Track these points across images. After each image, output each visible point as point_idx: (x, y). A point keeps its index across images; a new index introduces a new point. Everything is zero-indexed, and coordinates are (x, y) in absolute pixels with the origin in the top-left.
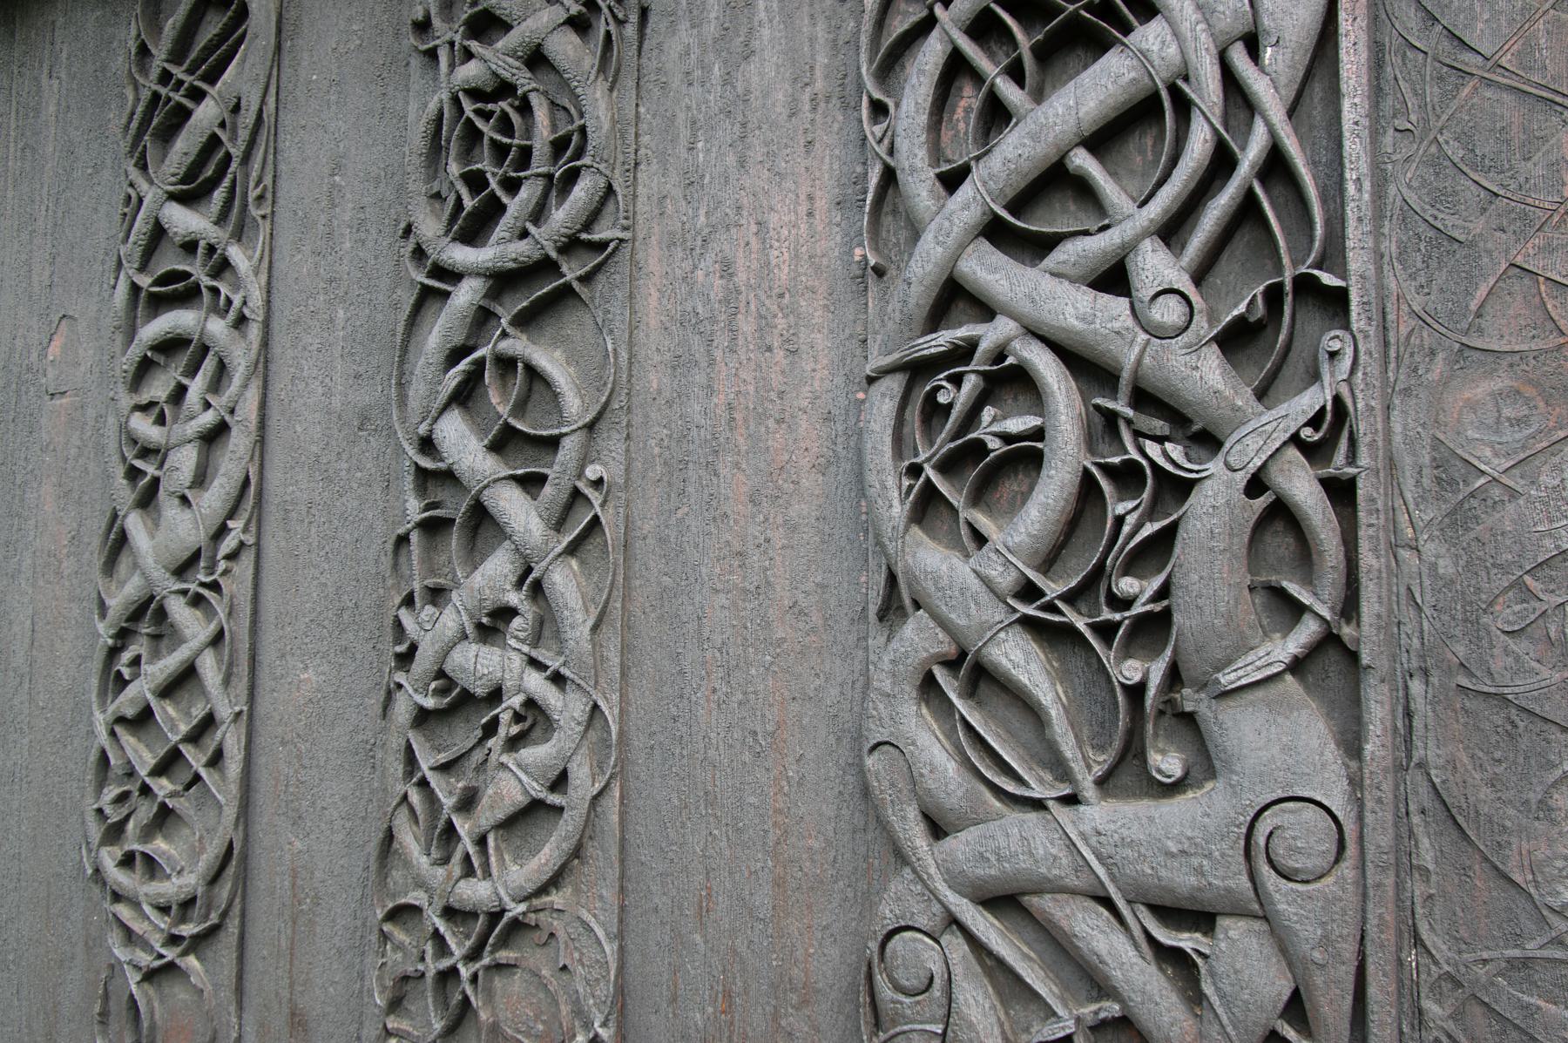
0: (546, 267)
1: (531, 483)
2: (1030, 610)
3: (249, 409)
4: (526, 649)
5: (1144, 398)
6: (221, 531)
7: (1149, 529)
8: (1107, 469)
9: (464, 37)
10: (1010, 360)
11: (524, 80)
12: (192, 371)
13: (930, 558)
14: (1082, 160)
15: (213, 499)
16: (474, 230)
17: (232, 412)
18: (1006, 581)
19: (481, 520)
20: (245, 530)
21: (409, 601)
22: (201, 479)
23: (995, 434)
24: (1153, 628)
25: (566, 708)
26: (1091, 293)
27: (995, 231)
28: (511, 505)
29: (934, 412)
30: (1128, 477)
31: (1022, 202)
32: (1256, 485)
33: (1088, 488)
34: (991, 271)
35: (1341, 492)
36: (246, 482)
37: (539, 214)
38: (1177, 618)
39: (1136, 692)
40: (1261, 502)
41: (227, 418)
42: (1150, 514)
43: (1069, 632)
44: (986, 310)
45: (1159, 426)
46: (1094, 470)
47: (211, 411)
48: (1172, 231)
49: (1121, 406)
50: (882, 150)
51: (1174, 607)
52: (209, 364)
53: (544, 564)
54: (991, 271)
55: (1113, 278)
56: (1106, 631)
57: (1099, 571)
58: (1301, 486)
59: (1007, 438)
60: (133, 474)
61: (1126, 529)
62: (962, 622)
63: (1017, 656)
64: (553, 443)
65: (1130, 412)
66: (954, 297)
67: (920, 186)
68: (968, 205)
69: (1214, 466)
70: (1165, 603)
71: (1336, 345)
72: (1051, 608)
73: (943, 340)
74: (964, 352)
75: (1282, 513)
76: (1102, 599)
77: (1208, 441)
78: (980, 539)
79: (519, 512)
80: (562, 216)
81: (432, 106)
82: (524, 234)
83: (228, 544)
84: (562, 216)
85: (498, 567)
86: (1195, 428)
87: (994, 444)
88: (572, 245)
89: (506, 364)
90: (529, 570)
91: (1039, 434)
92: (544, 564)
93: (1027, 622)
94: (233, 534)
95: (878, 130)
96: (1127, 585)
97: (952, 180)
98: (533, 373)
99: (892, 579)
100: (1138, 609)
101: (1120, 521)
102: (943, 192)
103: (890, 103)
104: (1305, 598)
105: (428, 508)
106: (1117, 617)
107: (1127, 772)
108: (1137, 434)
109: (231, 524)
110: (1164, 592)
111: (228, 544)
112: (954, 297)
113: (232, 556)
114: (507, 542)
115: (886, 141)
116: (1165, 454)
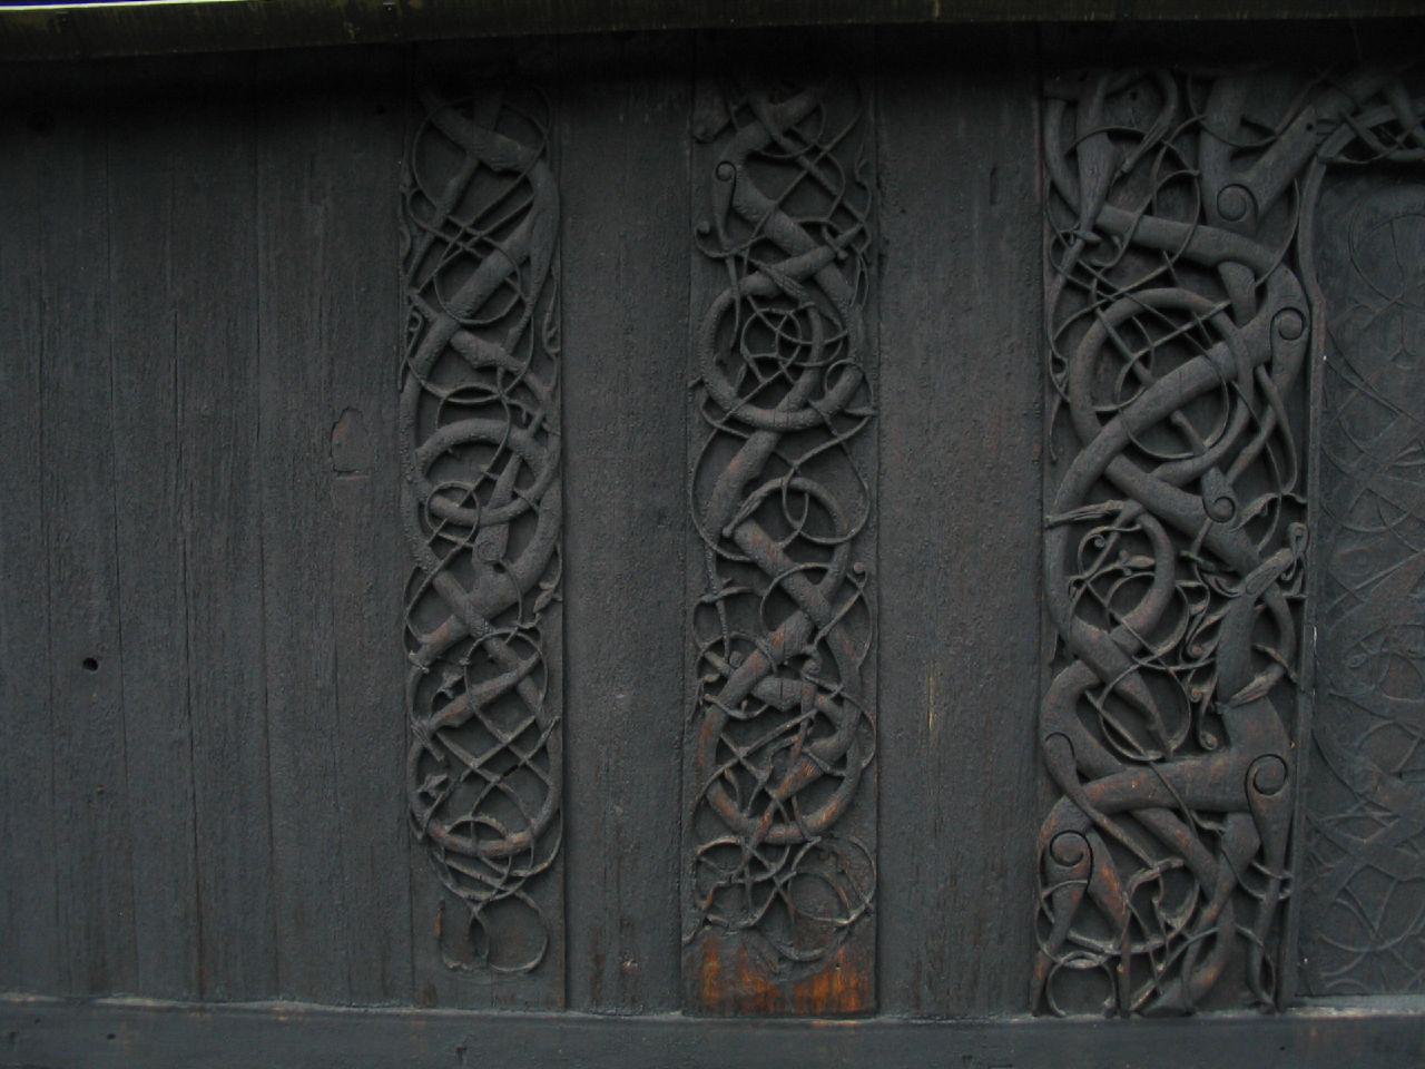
0: (821, 429)
1: (816, 574)
2: (1144, 662)
3: (553, 498)
4: (817, 681)
5: (1206, 551)
6: (535, 590)
7: (1207, 623)
8: (1187, 589)
9: (751, 254)
10: (1138, 527)
11: (807, 301)
12: (497, 467)
13: (1088, 631)
14: (1179, 418)
15: (526, 562)
16: (765, 399)
17: (538, 503)
18: (1133, 646)
19: (783, 599)
20: (556, 590)
21: (718, 647)
22: (511, 550)
23: (1129, 567)
24: (1205, 673)
25: (846, 717)
26: (1183, 494)
27: (1130, 450)
28: (800, 587)
29: (1092, 550)
30: (1197, 594)
31: (1144, 433)
32: (1260, 600)
33: (1176, 602)
34: (1123, 469)
35: (1295, 604)
36: (555, 553)
37: (817, 392)
38: (1220, 668)
39: (1196, 706)
40: (1260, 607)
41: (536, 507)
42: (1210, 611)
43: (1165, 674)
44: (1120, 492)
45: (1211, 565)
46: (1182, 591)
47: (519, 501)
48: (1224, 463)
49: (1193, 555)
50: (1062, 390)
51: (1217, 662)
52: (512, 464)
53: (827, 628)
54: (1123, 469)
55: (1193, 485)
56: (1182, 674)
57: (1182, 644)
58: (1278, 600)
59: (1135, 570)
60: (438, 543)
61: (1196, 622)
62: (1108, 669)
63: (1139, 689)
64: (830, 549)
65: (1200, 560)
66: (1105, 484)
67: (1084, 414)
68: (1111, 433)
69: (1238, 590)
70: (1212, 659)
71: (1298, 533)
72: (1156, 662)
73: (1095, 510)
74: (1110, 517)
75: (1268, 617)
76: (1180, 657)
77: (1236, 577)
78: (1115, 623)
79: (814, 595)
80: (834, 396)
81: (723, 297)
82: (806, 406)
83: (541, 601)
84: (834, 396)
85: (791, 628)
86: (1231, 569)
87: (1128, 573)
88: (842, 415)
89: (796, 493)
90: (815, 631)
91: (1152, 568)
92: (827, 628)
93: (1142, 671)
94: (543, 595)
95: (1060, 376)
96: (1194, 650)
97: (1104, 418)
98: (815, 500)
99: (1061, 642)
100: (1200, 664)
101: (1192, 618)
102: (1099, 424)
103: (1065, 360)
104: (1278, 657)
105: (729, 584)
106: (1190, 666)
107: (1194, 745)
108: (1202, 571)
109: (543, 585)
110: (1213, 654)
111: (541, 601)
112: (1105, 484)
113: (545, 610)
114: (799, 613)
115: (1064, 385)
116: (1217, 582)
